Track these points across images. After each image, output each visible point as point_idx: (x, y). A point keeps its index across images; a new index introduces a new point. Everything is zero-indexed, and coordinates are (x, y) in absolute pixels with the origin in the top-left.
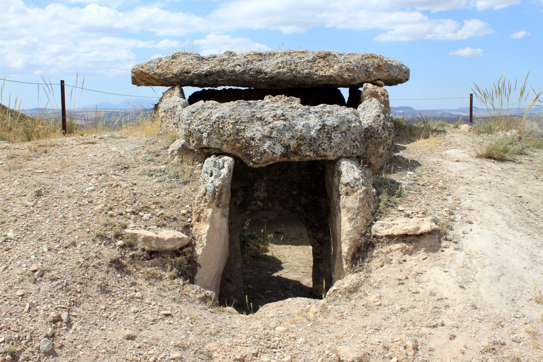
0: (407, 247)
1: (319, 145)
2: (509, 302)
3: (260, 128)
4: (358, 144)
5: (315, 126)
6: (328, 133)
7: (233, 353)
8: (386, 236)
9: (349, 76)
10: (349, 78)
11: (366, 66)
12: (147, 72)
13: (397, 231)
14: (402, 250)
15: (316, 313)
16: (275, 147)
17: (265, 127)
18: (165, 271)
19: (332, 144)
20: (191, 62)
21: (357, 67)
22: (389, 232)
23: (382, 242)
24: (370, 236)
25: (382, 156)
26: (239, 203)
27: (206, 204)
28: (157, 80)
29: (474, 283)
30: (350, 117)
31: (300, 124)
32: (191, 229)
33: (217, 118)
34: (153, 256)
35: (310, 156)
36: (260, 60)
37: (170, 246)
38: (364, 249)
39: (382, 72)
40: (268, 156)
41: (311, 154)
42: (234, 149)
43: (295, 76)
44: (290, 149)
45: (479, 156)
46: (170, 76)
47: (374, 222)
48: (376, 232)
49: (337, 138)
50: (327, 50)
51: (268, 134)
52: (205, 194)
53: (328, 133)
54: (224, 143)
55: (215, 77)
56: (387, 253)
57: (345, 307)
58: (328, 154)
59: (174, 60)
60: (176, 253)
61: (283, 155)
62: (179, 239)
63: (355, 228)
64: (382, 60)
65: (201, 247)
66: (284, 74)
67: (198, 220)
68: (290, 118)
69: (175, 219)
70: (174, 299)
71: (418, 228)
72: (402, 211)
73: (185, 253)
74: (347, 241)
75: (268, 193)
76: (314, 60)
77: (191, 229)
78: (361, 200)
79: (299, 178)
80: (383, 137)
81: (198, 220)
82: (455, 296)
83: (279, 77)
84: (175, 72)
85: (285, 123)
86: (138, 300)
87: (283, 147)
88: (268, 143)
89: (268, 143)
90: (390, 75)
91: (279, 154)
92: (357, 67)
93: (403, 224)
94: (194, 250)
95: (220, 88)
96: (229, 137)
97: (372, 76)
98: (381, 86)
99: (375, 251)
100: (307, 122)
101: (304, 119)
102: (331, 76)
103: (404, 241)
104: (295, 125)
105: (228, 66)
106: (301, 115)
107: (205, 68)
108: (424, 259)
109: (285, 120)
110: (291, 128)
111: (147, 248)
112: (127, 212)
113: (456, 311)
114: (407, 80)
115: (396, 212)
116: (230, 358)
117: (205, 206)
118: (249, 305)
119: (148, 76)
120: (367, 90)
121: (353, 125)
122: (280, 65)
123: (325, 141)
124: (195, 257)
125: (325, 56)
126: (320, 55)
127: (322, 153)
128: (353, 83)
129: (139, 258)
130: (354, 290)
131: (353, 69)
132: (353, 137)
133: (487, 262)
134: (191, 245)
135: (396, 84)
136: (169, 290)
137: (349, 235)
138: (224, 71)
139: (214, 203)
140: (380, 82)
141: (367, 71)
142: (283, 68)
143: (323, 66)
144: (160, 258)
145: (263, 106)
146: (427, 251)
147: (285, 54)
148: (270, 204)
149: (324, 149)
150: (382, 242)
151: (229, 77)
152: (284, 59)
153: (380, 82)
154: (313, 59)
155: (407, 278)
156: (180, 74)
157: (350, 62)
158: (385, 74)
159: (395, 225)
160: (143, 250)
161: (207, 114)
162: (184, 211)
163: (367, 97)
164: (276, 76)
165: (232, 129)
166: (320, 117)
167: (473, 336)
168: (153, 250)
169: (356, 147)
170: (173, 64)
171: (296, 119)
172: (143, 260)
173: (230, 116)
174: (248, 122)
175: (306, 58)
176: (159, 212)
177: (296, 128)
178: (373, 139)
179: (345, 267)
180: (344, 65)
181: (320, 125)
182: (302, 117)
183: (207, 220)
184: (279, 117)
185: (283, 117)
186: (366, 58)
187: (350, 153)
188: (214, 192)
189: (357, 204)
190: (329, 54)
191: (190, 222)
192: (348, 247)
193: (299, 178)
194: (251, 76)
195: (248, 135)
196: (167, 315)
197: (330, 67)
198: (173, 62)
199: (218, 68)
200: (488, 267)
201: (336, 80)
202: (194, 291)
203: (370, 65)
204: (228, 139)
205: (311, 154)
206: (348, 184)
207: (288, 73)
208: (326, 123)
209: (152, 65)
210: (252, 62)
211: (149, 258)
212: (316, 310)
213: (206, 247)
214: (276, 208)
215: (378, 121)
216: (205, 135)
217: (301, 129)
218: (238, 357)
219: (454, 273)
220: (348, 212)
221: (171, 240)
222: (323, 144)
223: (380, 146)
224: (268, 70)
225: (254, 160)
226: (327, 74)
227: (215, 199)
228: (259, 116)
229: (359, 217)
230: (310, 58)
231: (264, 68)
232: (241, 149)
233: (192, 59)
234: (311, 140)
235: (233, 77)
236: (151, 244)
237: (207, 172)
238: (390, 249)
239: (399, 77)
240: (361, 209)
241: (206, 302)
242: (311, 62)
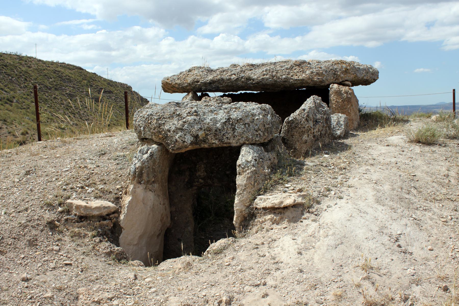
0: (275, 217)
1: (223, 134)
2: (336, 268)
4: (261, 133)
5: (221, 119)
6: (232, 125)
7: (94, 296)
9: (318, 79)
10: (318, 80)
12: (170, 83)
13: (268, 204)
14: (271, 220)
15: (180, 269)
16: (185, 137)
18: (88, 231)
19: (236, 134)
21: (326, 72)
23: (261, 213)
25: (306, 142)
26: (186, 180)
28: (178, 89)
29: (313, 250)
30: (255, 111)
31: (208, 119)
33: (148, 115)
34: (83, 220)
36: (251, 70)
37: (96, 213)
39: (349, 75)
41: (217, 142)
43: (276, 81)
44: (199, 138)
45: (411, 142)
46: (186, 85)
48: (256, 204)
49: (240, 128)
53: (232, 125)
55: (216, 84)
56: (263, 222)
58: (231, 141)
59: (190, 73)
60: (102, 218)
62: (105, 208)
66: (267, 79)
69: (110, 192)
70: (84, 252)
71: (282, 202)
73: (111, 218)
75: (207, 173)
76: (291, 68)
78: (249, 178)
80: (306, 127)
82: (289, 261)
83: (263, 82)
84: (189, 82)
85: (195, 117)
86: (55, 252)
87: (193, 136)
88: (180, 134)
89: (180, 134)
90: (356, 76)
91: (189, 142)
94: (119, 216)
95: (239, 92)
96: (154, 130)
97: (340, 78)
98: (349, 86)
99: (256, 220)
100: (216, 116)
101: (213, 114)
102: (303, 80)
104: (205, 119)
106: (211, 111)
108: (284, 228)
109: (197, 115)
110: (200, 121)
112: (77, 187)
113: (283, 273)
114: (375, 80)
116: (90, 300)
120: (332, 90)
122: (265, 73)
123: (229, 132)
126: (296, 63)
127: (226, 140)
128: (323, 84)
129: (72, 221)
131: (322, 73)
132: (256, 127)
133: (331, 232)
134: (117, 212)
140: (347, 83)
141: (335, 74)
142: (266, 75)
146: (289, 221)
148: (210, 182)
149: (227, 138)
150: (261, 213)
151: (227, 84)
153: (347, 83)
155: (263, 244)
156: (192, 83)
158: (352, 76)
160: (75, 215)
165: (156, 123)
167: (284, 295)
168: (82, 215)
169: (259, 136)
172: (74, 222)
173: (156, 113)
175: (286, 67)
176: (101, 187)
177: (205, 121)
178: (297, 128)
186: (335, 64)
187: (252, 140)
188: (135, 172)
189: (245, 182)
190: (304, 62)
191: (121, 195)
194: (243, 82)
196: (66, 264)
197: (303, 72)
199: (219, 77)
200: (330, 237)
201: (307, 83)
202: (103, 248)
205: (217, 142)
207: (270, 78)
213: (126, 214)
214: (216, 184)
215: (303, 114)
216: (142, 128)
218: (96, 300)
219: (299, 240)
221: (97, 208)
222: (227, 134)
223: (304, 134)
227: (135, 177)
229: (245, 192)
230: (289, 66)
233: (202, 72)
235: (230, 84)
241: (110, 256)
242: (289, 69)
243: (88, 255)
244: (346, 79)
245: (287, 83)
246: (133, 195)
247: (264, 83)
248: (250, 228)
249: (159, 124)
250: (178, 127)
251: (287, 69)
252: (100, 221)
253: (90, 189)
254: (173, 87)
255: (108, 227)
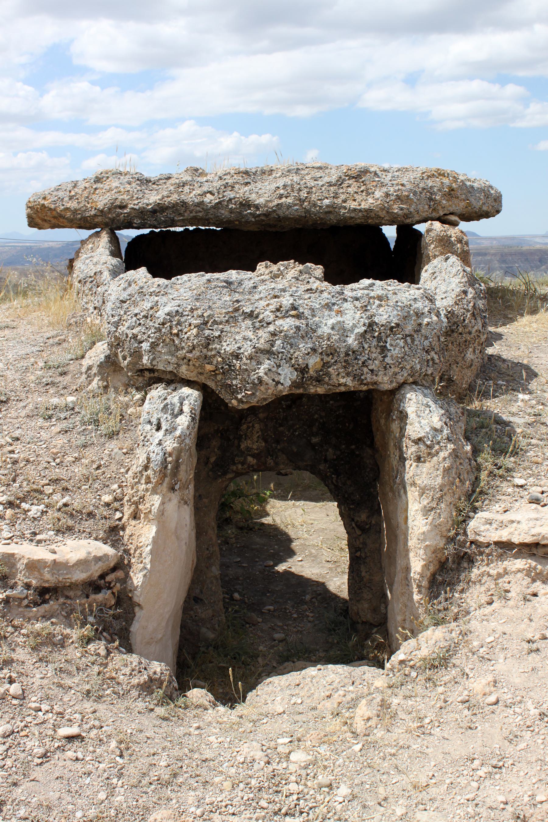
0: (539, 567)
1: (363, 363)
3: (250, 334)
4: (436, 357)
5: (354, 326)
6: (379, 339)
8: (497, 543)
9: (402, 209)
11: (430, 191)
12: (53, 206)
15: (369, 719)
16: (280, 371)
17: (260, 333)
18: (71, 626)
19: (388, 360)
20: (128, 187)
21: (415, 193)
22: (504, 535)
23: (488, 555)
24: (465, 542)
25: (471, 365)
26: (212, 460)
27: (150, 486)
30: (419, 305)
31: (327, 323)
32: (121, 533)
33: (168, 314)
34: (47, 597)
35: (345, 385)
36: (247, 184)
37: (79, 576)
38: (453, 565)
39: (456, 201)
40: (267, 389)
42: (201, 374)
43: (307, 211)
44: (307, 372)
46: (93, 212)
47: (471, 514)
49: (396, 348)
50: (362, 164)
51: (267, 346)
52: (146, 468)
53: (379, 339)
54: (181, 362)
55: (169, 214)
56: (500, 576)
57: (423, 701)
58: (380, 379)
59: (99, 185)
60: (93, 586)
61: (295, 384)
62: (98, 559)
63: (435, 527)
64: (455, 179)
65: (141, 570)
66: (289, 207)
67: (135, 516)
68: (307, 313)
69: (90, 515)
70: (88, 692)
72: (522, 486)
73: (110, 583)
74: (422, 552)
75: (266, 441)
76: (340, 182)
77: (121, 533)
78: (447, 471)
79: (323, 414)
80: (474, 330)
81: (135, 516)
83: (280, 213)
84: (100, 206)
85: (297, 323)
86: (15, 702)
87: (296, 369)
89: (266, 364)
90: (469, 204)
91: (288, 383)
92: (415, 193)
93: (531, 524)
94: (127, 575)
96: (191, 352)
97: (439, 207)
98: (454, 224)
99: (475, 571)
100: (339, 319)
101: (333, 313)
103: (532, 556)
104: (318, 326)
105: (192, 195)
106: (328, 306)
107: (152, 198)
109: (298, 317)
110: (309, 332)
111: (34, 582)
114: (498, 212)
115: (510, 490)
117: (147, 490)
118: (236, 685)
119: (54, 213)
120: (432, 234)
121: (426, 320)
122: (282, 192)
123: (374, 355)
124: (131, 591)
125: (359, 175)
126: (350, 173)
127: (369, 377)
129: (20, 603)
130: (440, 662)
131: (408, 196)
132: (427, 343)
134: (121, 566)
135: (478, 220)
136: (78, 669)
137: (424, 540)
138: (184, 204)
139: (165, 485)
141: (431, 199)
142: (286, 197)
143: (356, 193)
144: (62, 600)
145: (255, 287)
147: (289, 171)
148: (270, 462)
149: (372, 371)
150: (488, 555)
151: (194, 214)
152: (287, 180)
153: (453, 218)
154: (338, 181)
156: (110, 209)
157: (403, 185)
158: (463, 204)
159: (515, 525)
160: (28, 586)
161: (149, 305)
162: (107, 498)
163: (433, 246)
164: (274, 211)
165: (197, 336)
166: (365, 309)
168: (47, 585)
169: (431, 363)
170: (97, 192)
171: (318, 313)
172: (27, 606)
173: (192, 310)
174: (227, 321)
175: (327, 179)
176: (59, 499)
177: (319, 332)
178: (455, 335)
179: (416, 597)
180: (392, 189)
181: (364, 325)
182: (331, 310)
183: (151, 517)
184: (287, 312)
185: (294, 311)
186: (429, 177)
187: (420, 375)
188: (164, 462)
189: (439, 480)
190: (366, 171)
191: (120, 519)
192: (422, 563)
193: (323, 414)
194: (231, 211)
195: (228, 349)
196: (70, 738)
197: (368, 194)
198: (96, 189)
199: (174, 198)
202: (127, 671)
203: (435, 189)
204: (189, 355)
206: (420, 439)
207: (296, 205)
208: (376, 319)
209: (61, 194)
210: (233, 187)
211: (39, 601)
212: (368, 714)
213: (150, 571)
216: (145, 346)
217: (329, 334)
220: (421, 495)
221: (82, 563)
223: (467, 347)
224: (261, 201)
225: (239, 396)
226: (362, 206)
227: (165, 476)
228: (248, 310)
229: (443, 505)
230: (334, 179)
231: (253, 197)
232: (214, 373)
233: (129, 183)
234: (347, 355)
235: (200, 214)
236: (41, 575)
237: (150, 422)
238: (505, 569)
239: (485, 208)
240: (446, 490)
243: (100, 697)
244: (451, 209)
245: (332, 217)
246: (159, 522)
247: (281, 214)
248: (460, 588)
249: (207, 338)
250: (261, 346)
251: (330, 184)
252: (88, 597)
253: (34, 508)
254: (60, 216)
255: (103, 603)
